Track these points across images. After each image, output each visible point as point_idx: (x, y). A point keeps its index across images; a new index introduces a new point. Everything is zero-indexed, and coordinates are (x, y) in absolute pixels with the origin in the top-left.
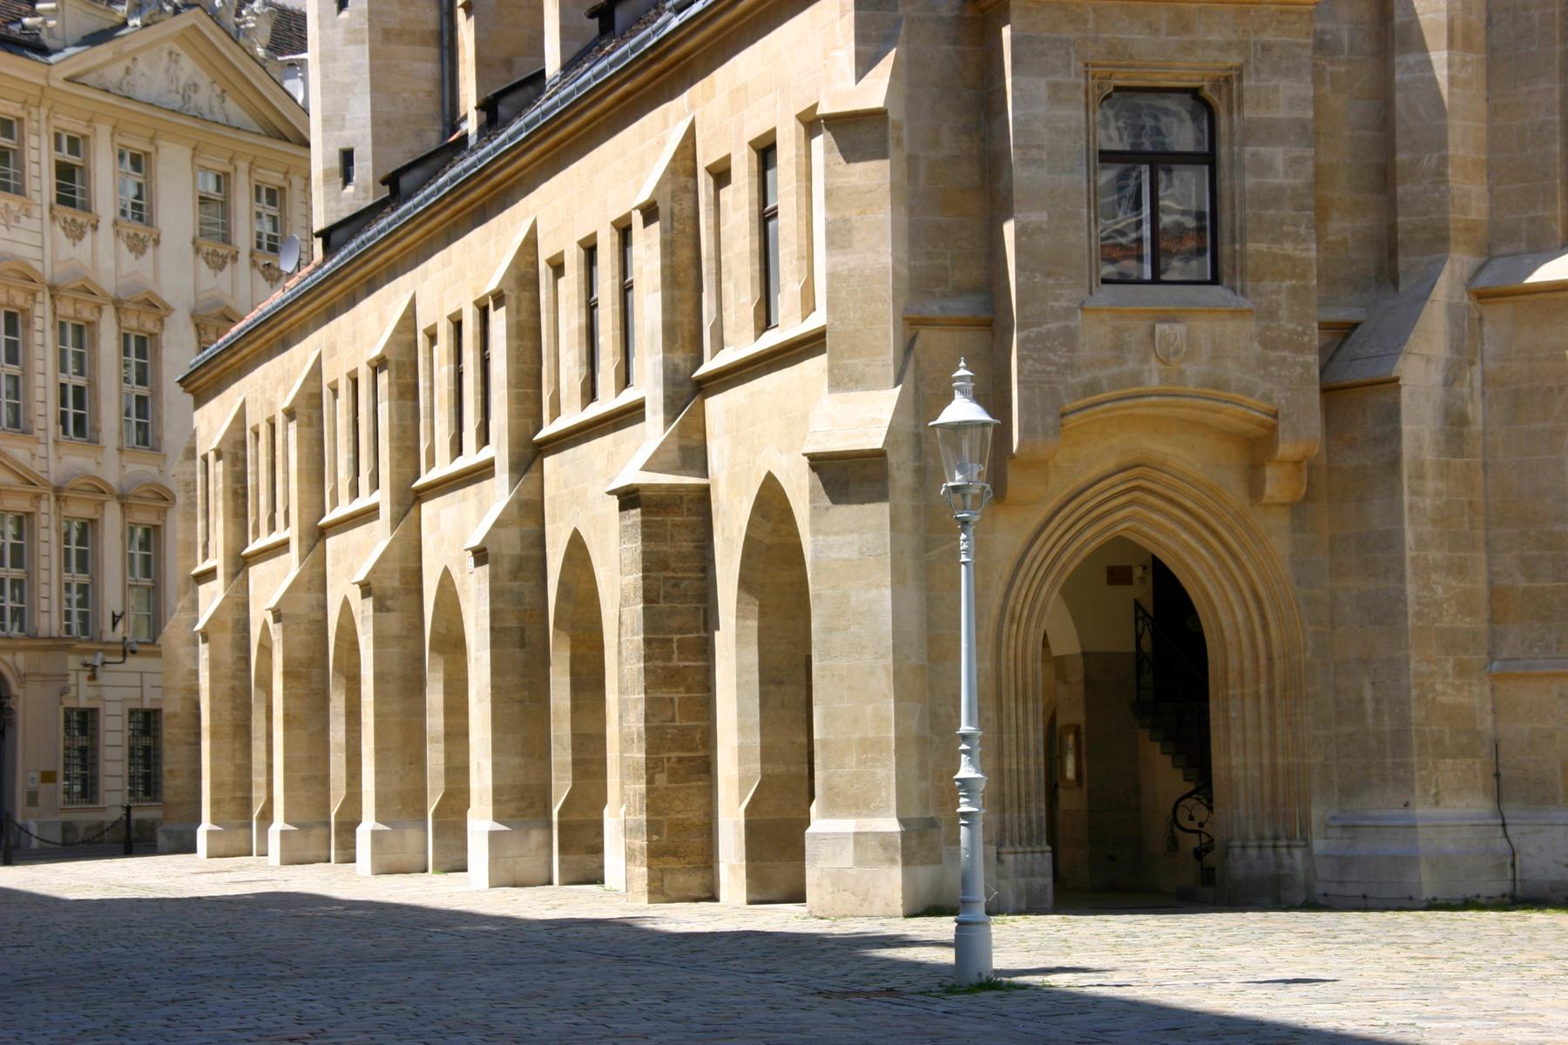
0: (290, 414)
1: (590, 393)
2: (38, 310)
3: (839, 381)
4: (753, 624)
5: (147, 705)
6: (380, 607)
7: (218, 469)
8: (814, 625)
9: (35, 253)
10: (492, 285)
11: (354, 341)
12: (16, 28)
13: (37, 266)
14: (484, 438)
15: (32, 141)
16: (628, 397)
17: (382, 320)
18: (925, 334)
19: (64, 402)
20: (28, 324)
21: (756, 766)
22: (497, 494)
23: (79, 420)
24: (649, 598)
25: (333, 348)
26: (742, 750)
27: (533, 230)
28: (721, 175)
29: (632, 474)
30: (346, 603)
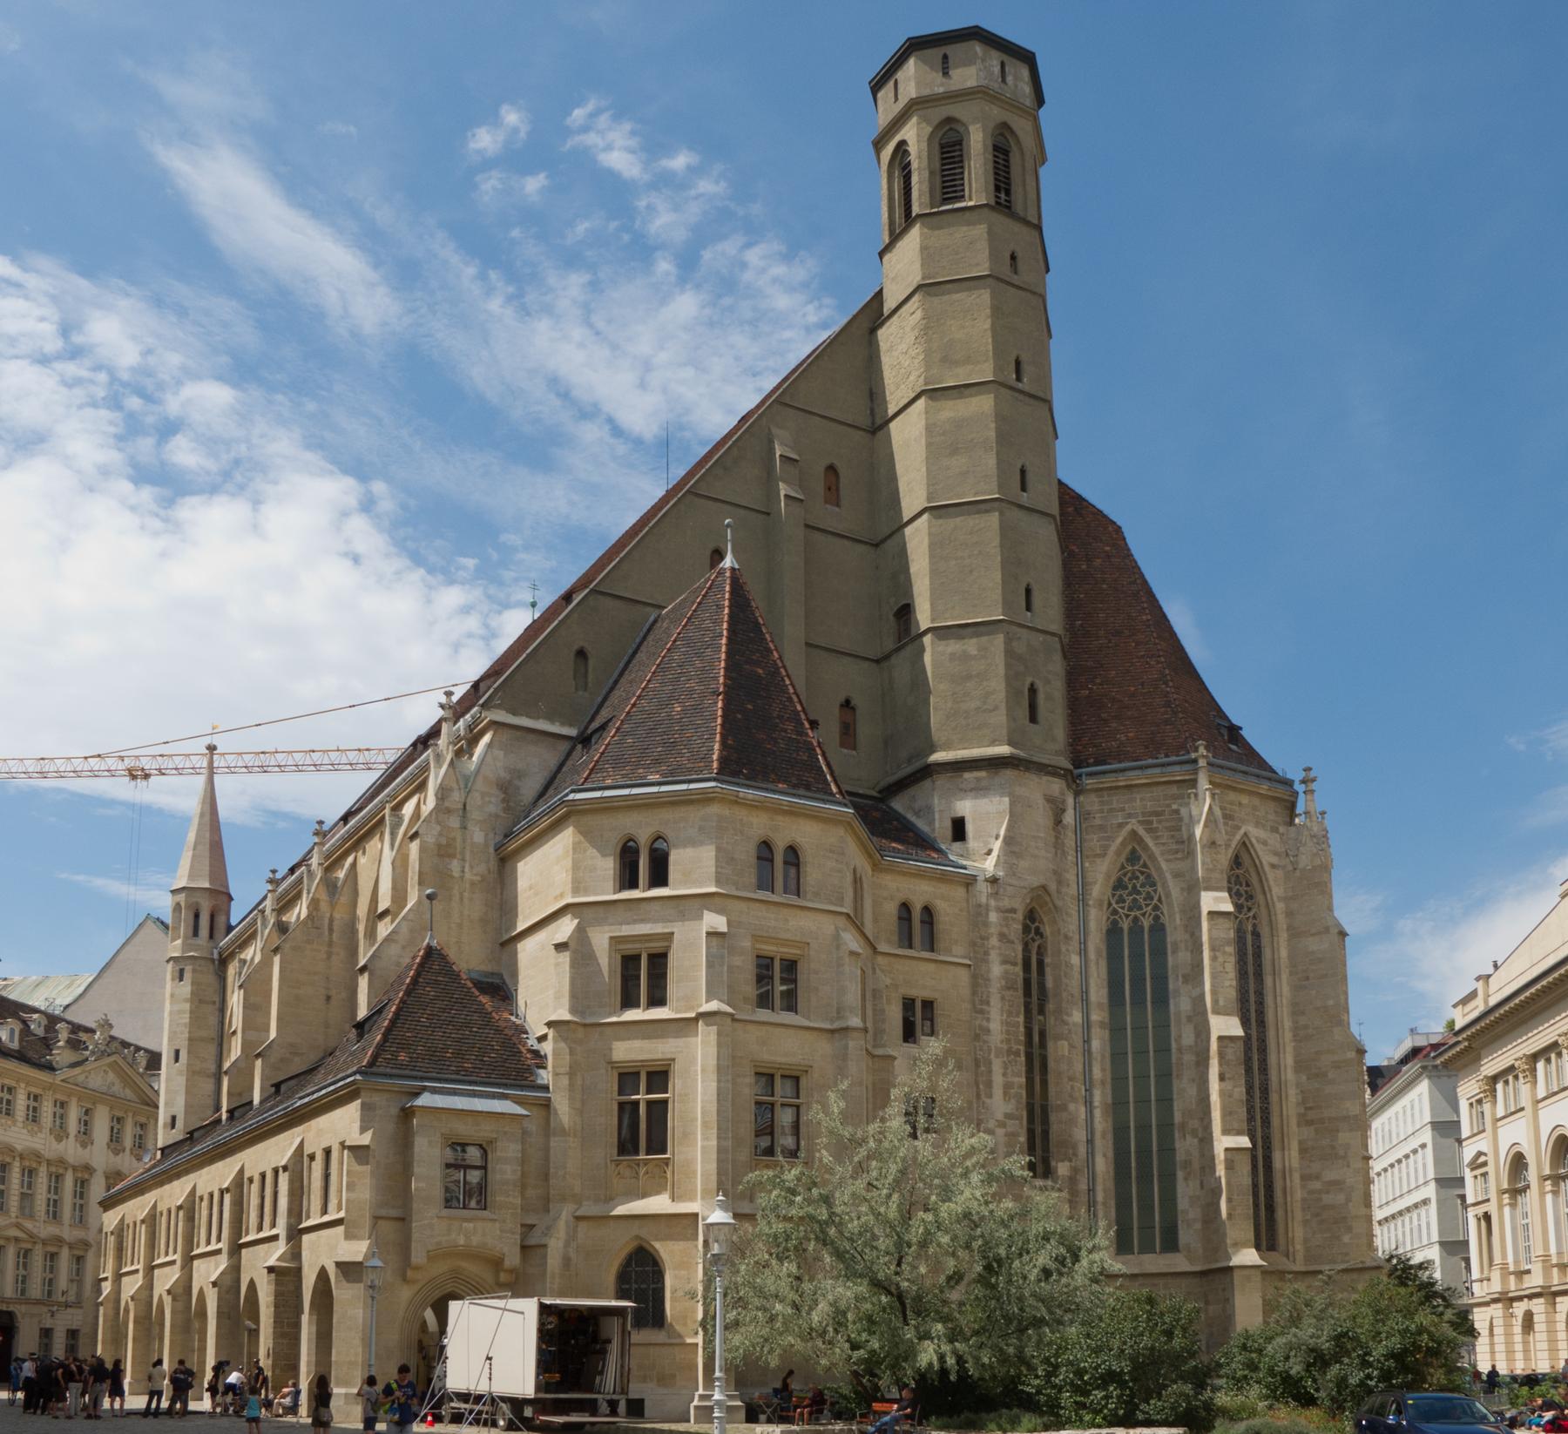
0: (143, 1221)
1: (260, 1229)
2: (41, 1169)
3: (349, 1236)
4: (315, 1317)
5: (74, 1327)
6: (174, 1299)
7: (111, 1239)
8: (334, 1321)
9: (43, 1147)
10: (225, 1185)
11: (170, 1196)
12: (43, 1060)
13: (43, 1152)
14: (219, 1240)
15: (46, 1103)
16: (274, 1232)
17: (182, 1191)
18: (380, 1222)
19: (48, 1206)
20: (37, 1175)
21: (313, 1368)
22: (223, 1263)
23: (55, 1213)
24: (276, 1306)
25: (162, 1198)
26: (309, 1363)
27: (243, 1167)
28: (312, 1157)
29: (272, 1262)
30: (161, 1296)
